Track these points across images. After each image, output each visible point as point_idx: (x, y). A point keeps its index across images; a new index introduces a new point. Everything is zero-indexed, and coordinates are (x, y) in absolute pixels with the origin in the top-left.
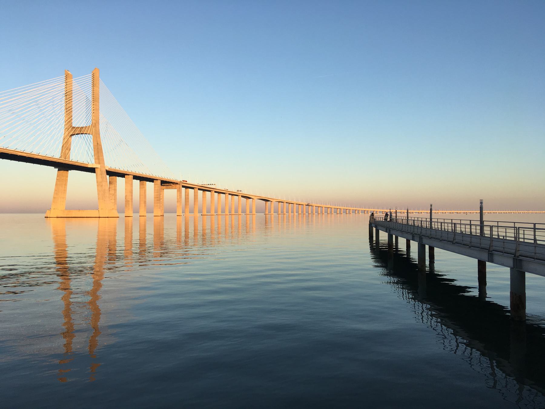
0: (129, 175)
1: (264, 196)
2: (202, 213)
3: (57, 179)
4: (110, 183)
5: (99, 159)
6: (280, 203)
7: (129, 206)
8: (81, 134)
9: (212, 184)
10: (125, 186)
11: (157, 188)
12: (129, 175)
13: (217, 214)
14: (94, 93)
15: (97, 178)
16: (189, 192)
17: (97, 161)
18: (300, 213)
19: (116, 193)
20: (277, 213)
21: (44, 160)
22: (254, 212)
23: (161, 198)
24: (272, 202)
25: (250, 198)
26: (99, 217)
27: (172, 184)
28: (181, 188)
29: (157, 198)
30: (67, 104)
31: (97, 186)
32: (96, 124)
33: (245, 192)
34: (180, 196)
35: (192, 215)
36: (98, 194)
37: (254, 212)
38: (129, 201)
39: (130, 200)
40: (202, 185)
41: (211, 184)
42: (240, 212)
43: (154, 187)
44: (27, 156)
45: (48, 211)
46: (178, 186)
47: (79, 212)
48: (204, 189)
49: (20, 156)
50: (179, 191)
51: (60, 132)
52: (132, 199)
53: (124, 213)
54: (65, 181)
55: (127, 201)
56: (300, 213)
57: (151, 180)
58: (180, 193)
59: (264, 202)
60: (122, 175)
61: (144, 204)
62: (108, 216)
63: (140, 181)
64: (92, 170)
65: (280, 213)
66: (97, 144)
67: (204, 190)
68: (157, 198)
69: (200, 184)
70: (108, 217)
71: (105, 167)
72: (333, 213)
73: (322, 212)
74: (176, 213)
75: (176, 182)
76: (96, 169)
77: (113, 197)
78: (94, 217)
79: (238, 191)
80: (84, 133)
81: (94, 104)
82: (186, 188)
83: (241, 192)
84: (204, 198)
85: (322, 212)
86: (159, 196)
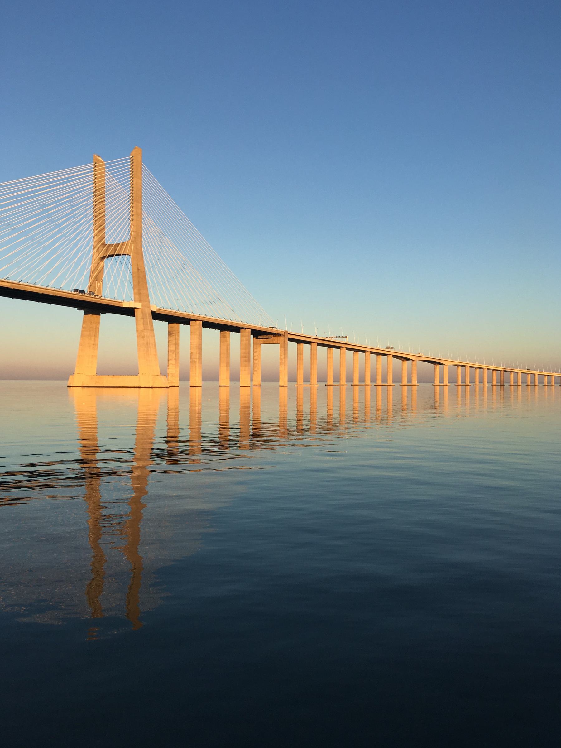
0: (195, 320)
1: (430, 357)
2: (326, 382)
3: (83, 328)
4: (170, 334)
5: (140, 294)
6: (460, 367)
7: (196, 371)
8: (117, 255)
9: (342, 337)
10: (191, 338)
11: (245, 342)
12: (195, 320)
13: (352, 384)
14: (133, 187)
15: (137, 325)
16: (303, 348)
17: (137, 297)
18: (495, 383)
19: (178, 349)
20: (432, 384)
21: (43, 294)
22: (415, 381)
24: (445, 366)
25: (408, 359)
26: (140, 387)
27: (272, 336)
28: (285, 343)
29: (245, 357)
30: (96, 209)
31: (137, 337)
32: (137, 237)
33: (400, 350)
34: (284, 355)
35: (307, 385)
36: (139, 349)
37: (415, 381)
38: (196, 362)
39: (197, 361)
40: (327, 337)
41: (339, 337)
42: (390, 381)
43: (241, 341)
44: (41, 292)
45: (71, 376)
46: (281, 338)
47: (112, 378)
48: (330, 345)
49: (29, 292)
50: (284, 348)
52: (200, 358)
53: (179, 381)
54: (94, 330)
55: (192, 362)
56: (495, 383)
57: (237, 329)
58: (284, 350)
59: (433, 365)
60: (186, 321)
61: (225, 368)
62: (152, 386)
63: (220, 332)
64: (130, 312)
65: (459, 383)
66: (136, 270)
67: (330, 347)
68: (245, 357)
69: (321, 336)
70: (151, 388)
71: (149, 307)
72: (553, 383)
73: (533, 382)
74: (278, 382)
75: (277, 333)
76: (135, 309)
77: (174, 355)
78: (133, 386)
79: (388, 348)
80: (122, 253)
81: (133, 205)
82: (298, 343)
83: (394, 349)
84: (329, 359)
85: (533, 382)
86: (247, 354)
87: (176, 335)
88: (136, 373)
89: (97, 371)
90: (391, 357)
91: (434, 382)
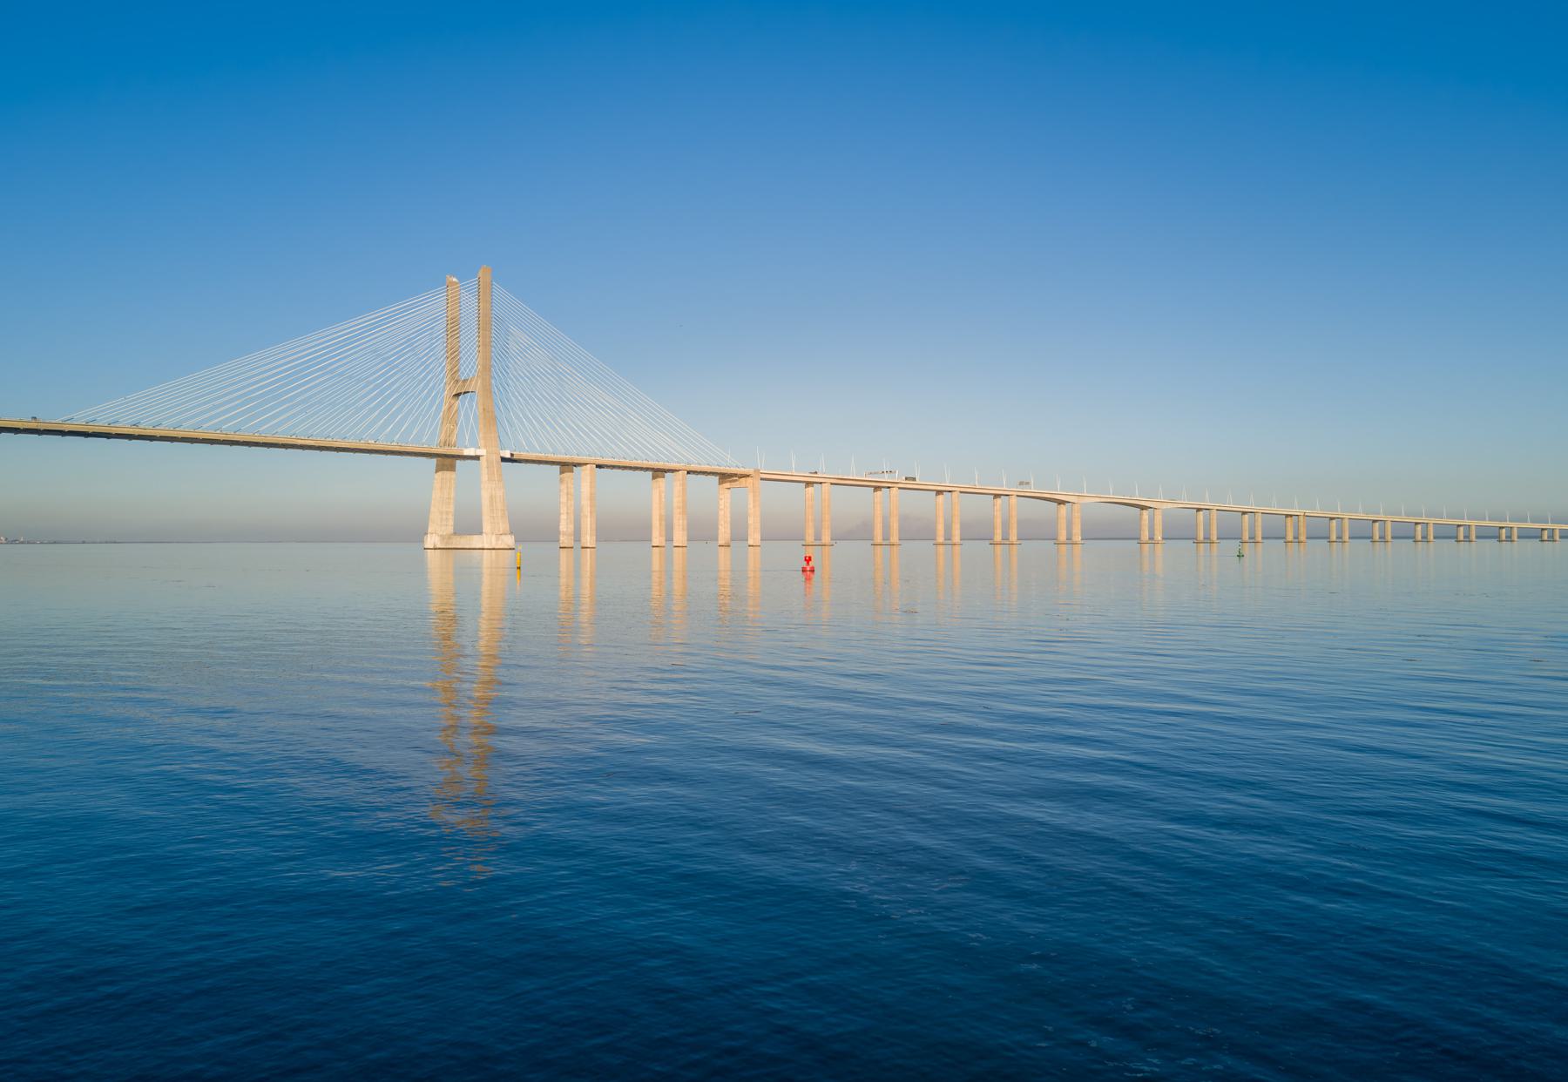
2: (872, 540)
8: (465, 393)
23: (721, 507)
26: (483, 549)
46: (749, 479)
51: (447, 391)
70: (494, 549)
87: (567, 483)
88: (481, 533)
89: (454, 529)
90: (1014, 500)
91: (1241, 539)
